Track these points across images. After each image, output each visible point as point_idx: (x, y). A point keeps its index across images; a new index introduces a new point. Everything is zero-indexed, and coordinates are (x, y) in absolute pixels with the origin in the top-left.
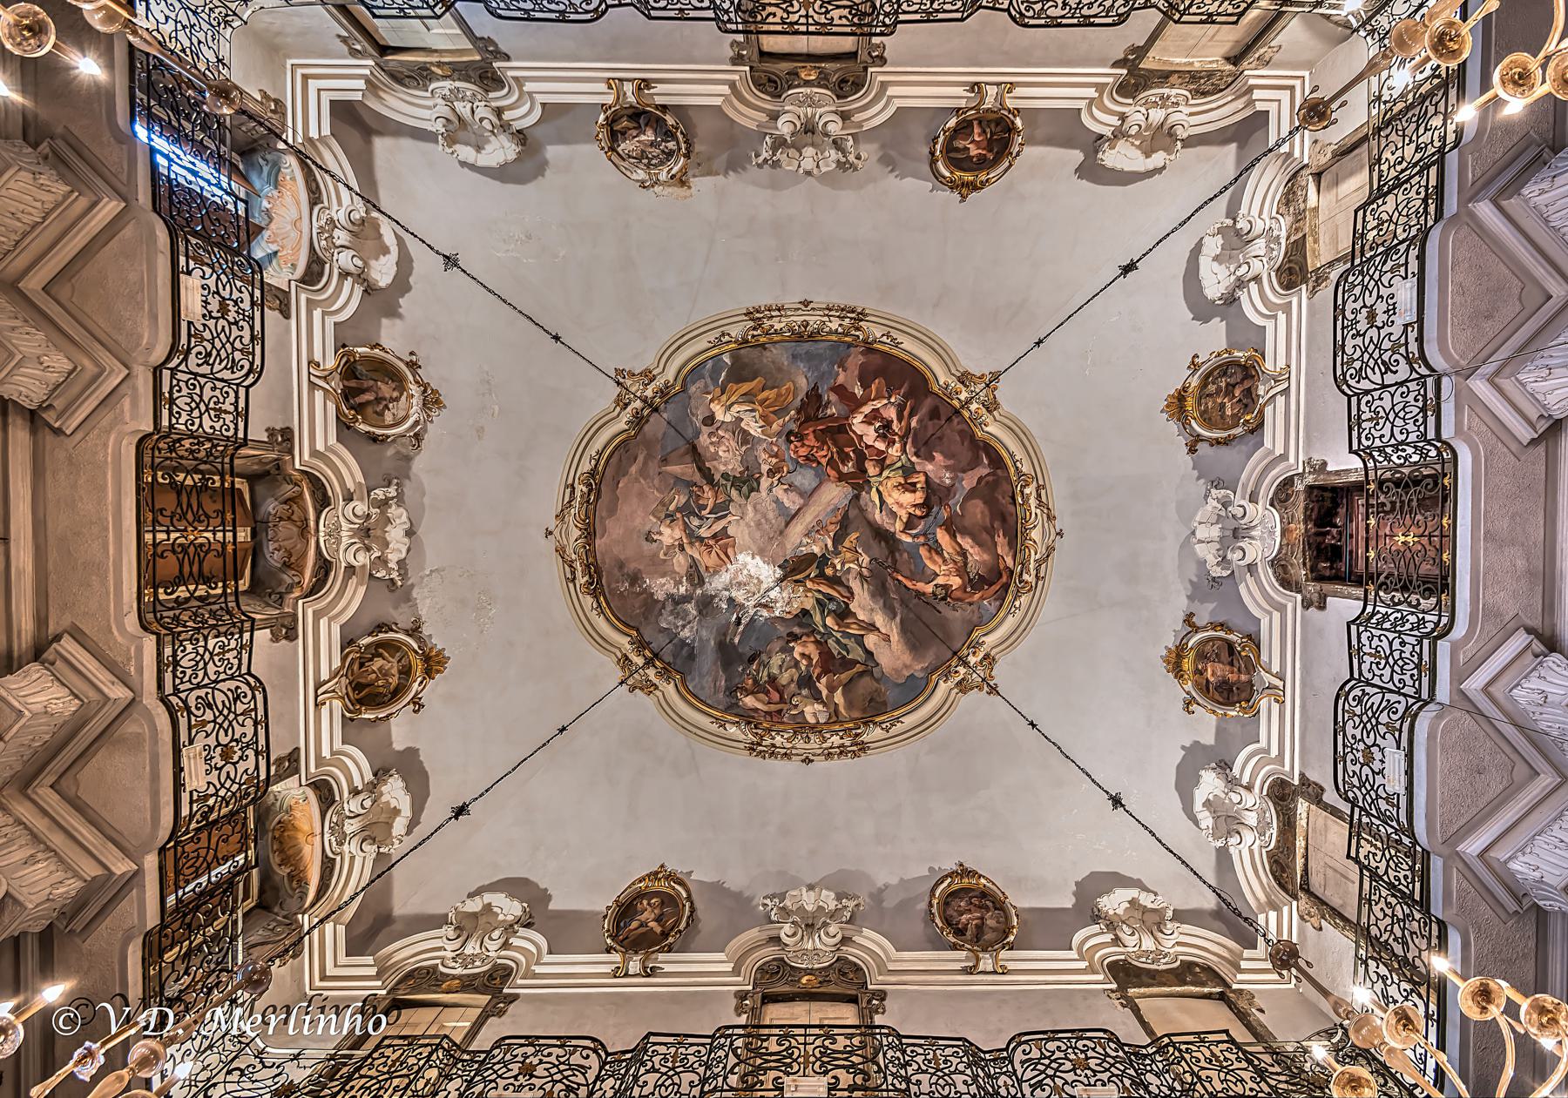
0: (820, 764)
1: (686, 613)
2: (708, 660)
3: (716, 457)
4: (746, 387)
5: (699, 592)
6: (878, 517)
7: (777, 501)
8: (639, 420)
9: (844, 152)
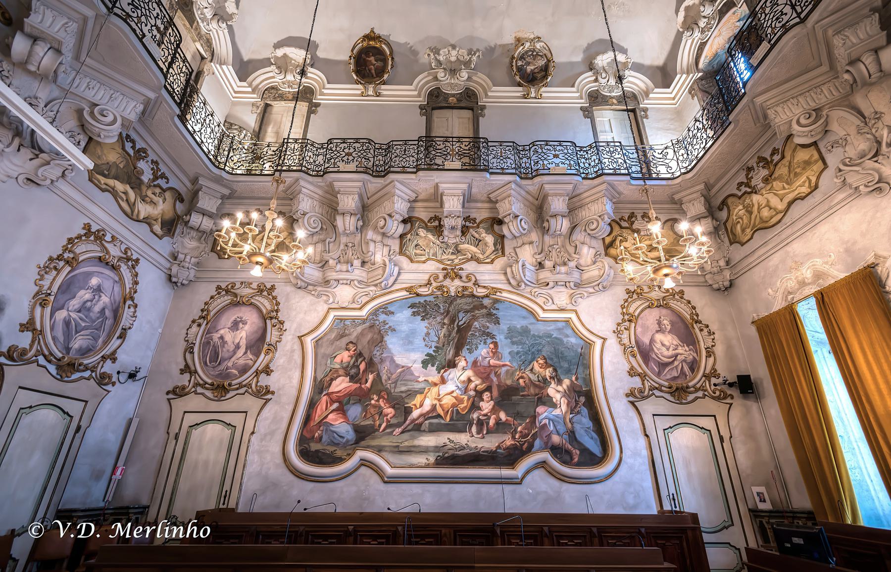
9: (436, 59)
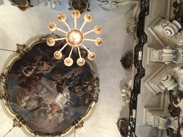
0: (100, 88)
1: (67, 114)
2: (78, 110)
3: (33, 106)
4: (18, 99)
5: (63, 111)
6: (49, 72)
7: (44, 93)
8: (24, 123)
